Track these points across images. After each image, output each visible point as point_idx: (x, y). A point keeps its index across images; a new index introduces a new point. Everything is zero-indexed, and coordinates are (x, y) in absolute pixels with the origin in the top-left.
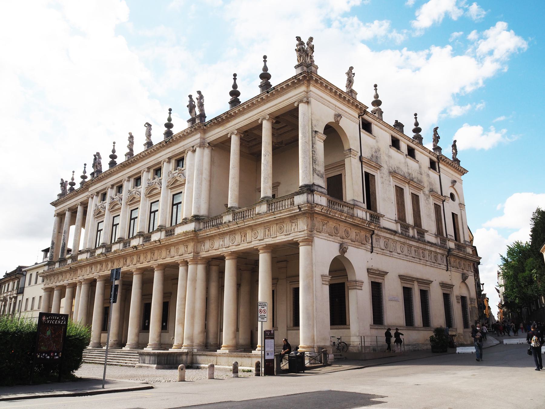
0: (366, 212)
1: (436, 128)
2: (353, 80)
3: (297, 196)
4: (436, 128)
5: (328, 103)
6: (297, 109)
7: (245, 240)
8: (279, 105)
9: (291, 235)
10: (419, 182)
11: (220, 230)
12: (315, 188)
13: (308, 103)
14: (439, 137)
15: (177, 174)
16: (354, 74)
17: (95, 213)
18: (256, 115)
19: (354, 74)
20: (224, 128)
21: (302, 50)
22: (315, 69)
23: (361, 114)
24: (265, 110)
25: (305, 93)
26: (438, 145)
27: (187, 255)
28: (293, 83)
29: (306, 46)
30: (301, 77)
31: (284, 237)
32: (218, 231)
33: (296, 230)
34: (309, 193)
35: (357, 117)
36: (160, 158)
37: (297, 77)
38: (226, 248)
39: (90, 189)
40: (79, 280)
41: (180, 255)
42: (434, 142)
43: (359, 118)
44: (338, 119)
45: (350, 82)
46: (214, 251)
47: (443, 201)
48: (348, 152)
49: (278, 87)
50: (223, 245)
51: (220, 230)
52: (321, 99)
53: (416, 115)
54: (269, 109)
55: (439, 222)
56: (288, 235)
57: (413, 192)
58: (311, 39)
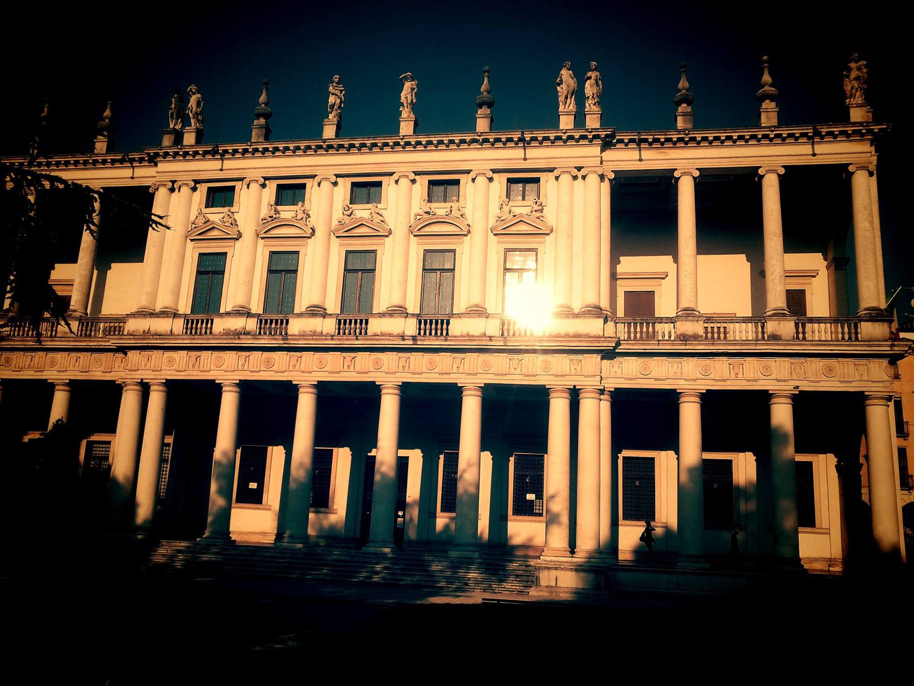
3: (866, 323)
7: (740, 376)
9: (853, 384)
11: (687, 347)
15: (529, 209)
17: (196, 230)
20: (661, 156)
27: (582, 378)
31: (838, 384)
32: (683, 347)
33: (865, 378)
36: (462, 163)
38: (686, 380)
39: (163, 166)
40: (142, 380)
41: (556, 376)
46: (653, 381)
50: (679, 374)
51: (687, 347)
56: (847, 382)
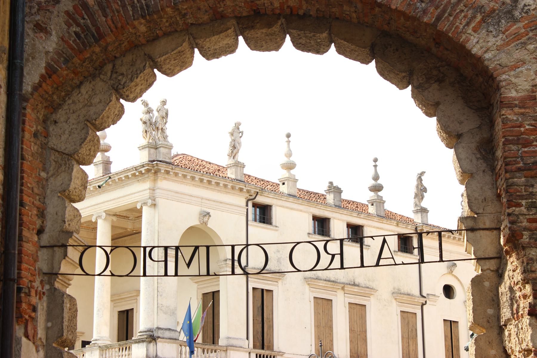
0: (250, 353)
1: (423, 173)
2: (240, 144)
4: (423, 173)
5: (188, 197)
6: (140, 211)
8: (118, 200)
10: (369, 281)
12: (160, 334)
13: (154, 205)
14: (425, 190)
16: (242, 132)
18: (88, 207)
19: (242, 132)
21: (148, 123)
22: (167, 150)
23: (251, 198)
24: (101, 203)
25: (151, 191)
26: (424, 204)
28: (134, 175)
29: (156, 114)
30: (143, 170)
34: (150, 342)
35: (244, 204)
37: (138, 169)
42: (416, 199)
43: (247, 206)
44: (204, 219)
45: (234, 148)
47: (423, 305)
48: (223, 263)
49: (115, 177)
52: (176, 195)
53: (376, 160)
54: (106, 204)
55: (411, 343)
57: (353, 301)
58: (164, 103)
